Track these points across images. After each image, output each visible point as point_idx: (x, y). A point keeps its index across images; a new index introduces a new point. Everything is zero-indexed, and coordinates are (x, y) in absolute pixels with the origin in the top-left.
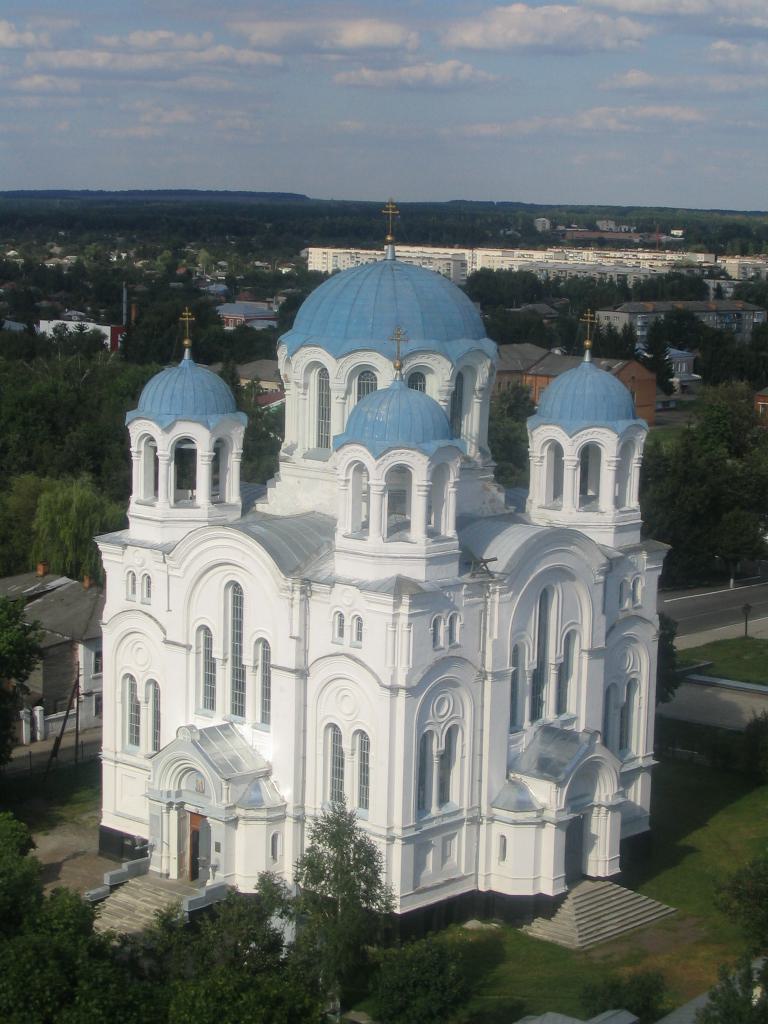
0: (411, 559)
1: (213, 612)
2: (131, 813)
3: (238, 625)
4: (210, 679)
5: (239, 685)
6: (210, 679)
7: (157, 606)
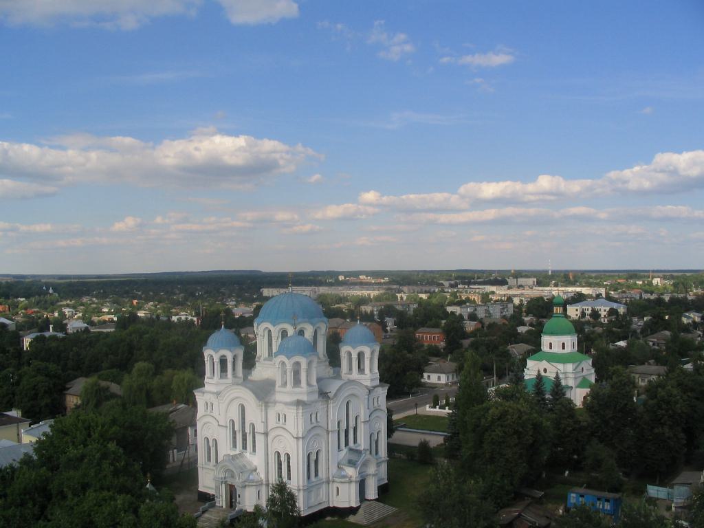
0: (302, 393)
1: (234, 414)
3: (243, 419)
4: (234, 438)
5: (244, 440)
6: (234, 438)
7: (215, 413)
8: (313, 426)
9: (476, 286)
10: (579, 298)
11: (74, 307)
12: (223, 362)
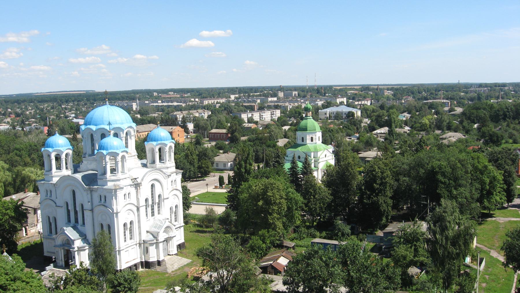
6: (69, 215)
7: (53, 198)
12: (58, 158)
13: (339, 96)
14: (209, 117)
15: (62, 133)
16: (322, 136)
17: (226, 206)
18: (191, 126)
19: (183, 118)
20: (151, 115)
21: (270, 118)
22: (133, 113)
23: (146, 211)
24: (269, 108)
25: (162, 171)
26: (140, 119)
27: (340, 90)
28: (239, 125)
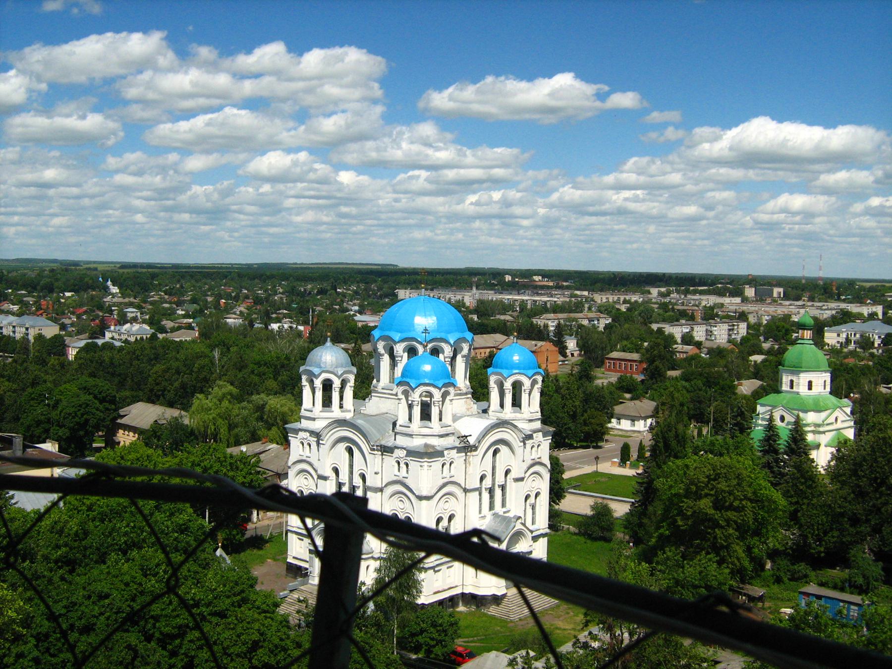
2: (302, 558)
3: (351, 466)
8: (445, 480)
9: (697, 297)
10: (844, 318)
11: (139, 307)
12: (327, 386)
13: (869, 301)
14: (607, 327)
15: (336, 340)
16: (832, 381)
17: (633, 502)
18: (571, 344)
19: (558, 326)
20: (498, 317)
21: (726, 337)
22: (465, 311)
23: (480, 500)
24: (727, 318)
25: (515, 427)
26: (477, 323)
27: (872, 289)
28: (665, 347)
